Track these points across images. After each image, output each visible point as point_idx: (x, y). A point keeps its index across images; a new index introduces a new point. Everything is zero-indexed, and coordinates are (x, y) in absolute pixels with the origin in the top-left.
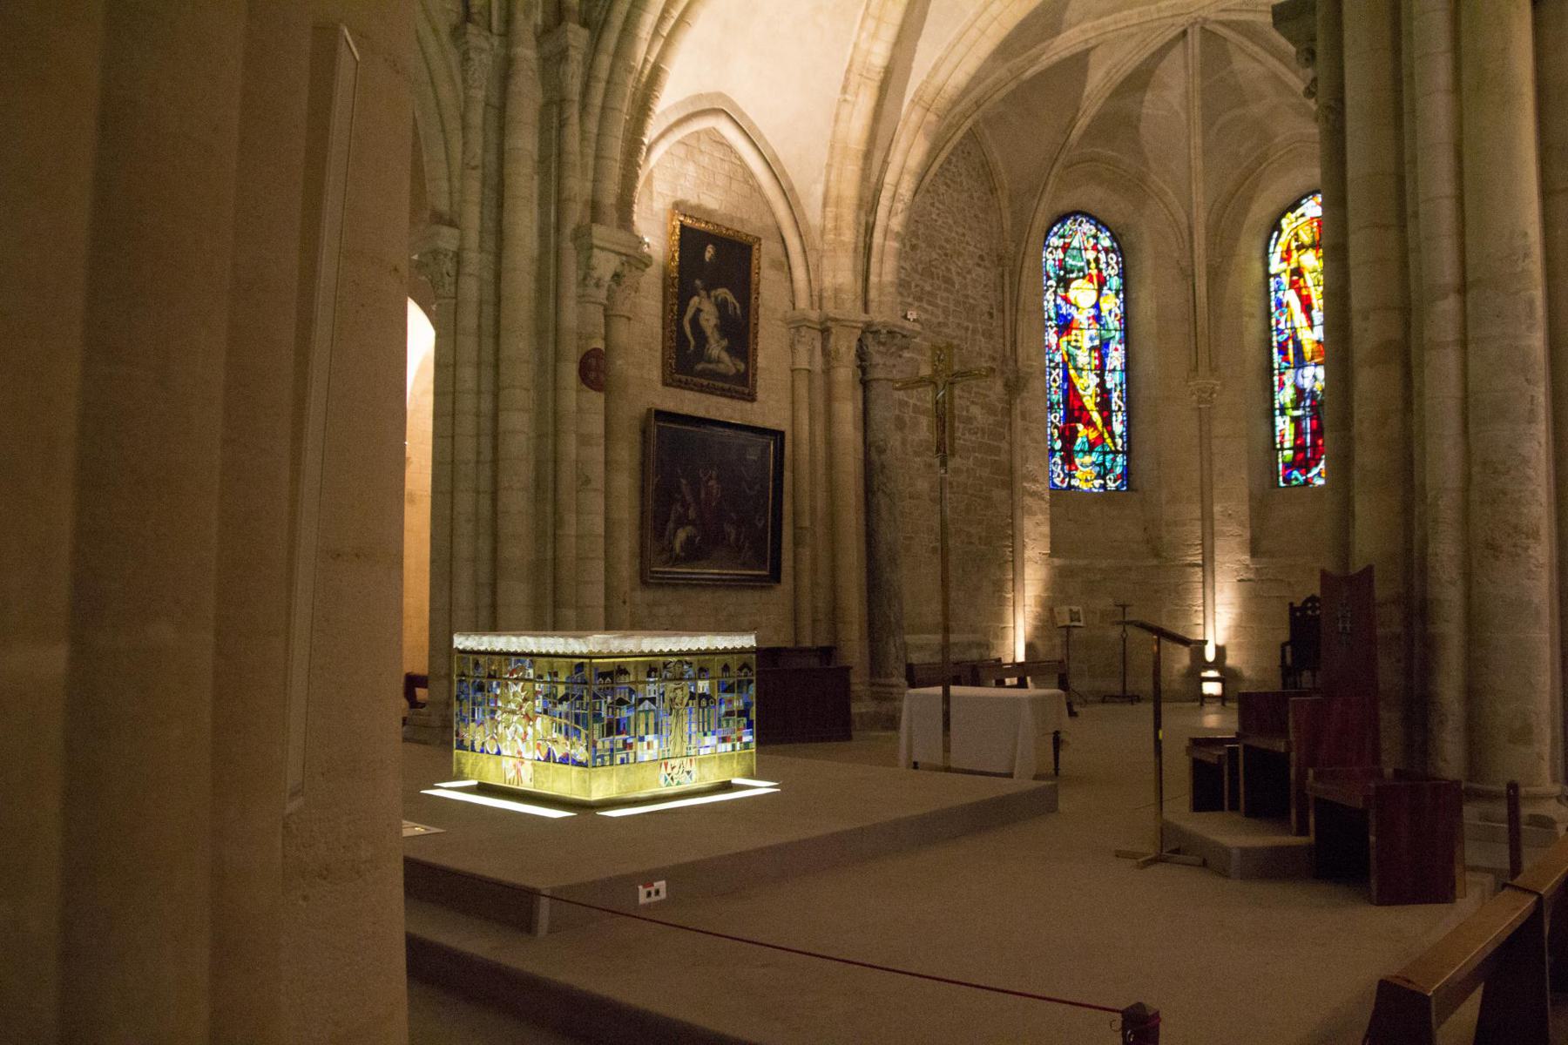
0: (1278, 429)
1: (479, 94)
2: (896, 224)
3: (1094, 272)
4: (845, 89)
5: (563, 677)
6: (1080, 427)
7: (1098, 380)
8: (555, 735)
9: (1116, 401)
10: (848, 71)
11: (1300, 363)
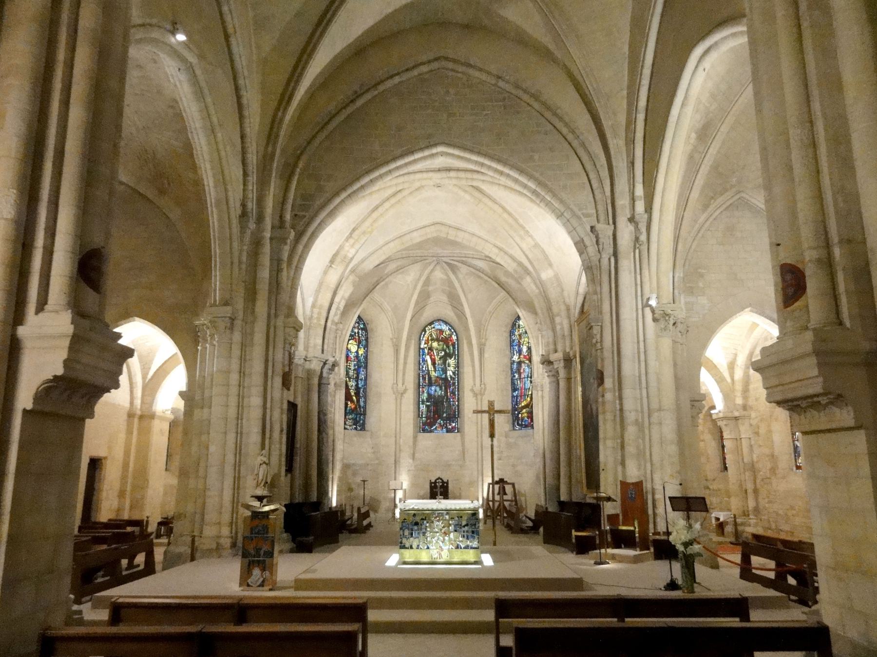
0: (421, 409)
1: (245, 248)
2: (337, 319)
3: (357, 338)
4: (332, 261)
5: (465, 517)
6: (349, 403)
7: (356, 383)
8: (461, 539)
10: (335, 255)
11: (430, 384)
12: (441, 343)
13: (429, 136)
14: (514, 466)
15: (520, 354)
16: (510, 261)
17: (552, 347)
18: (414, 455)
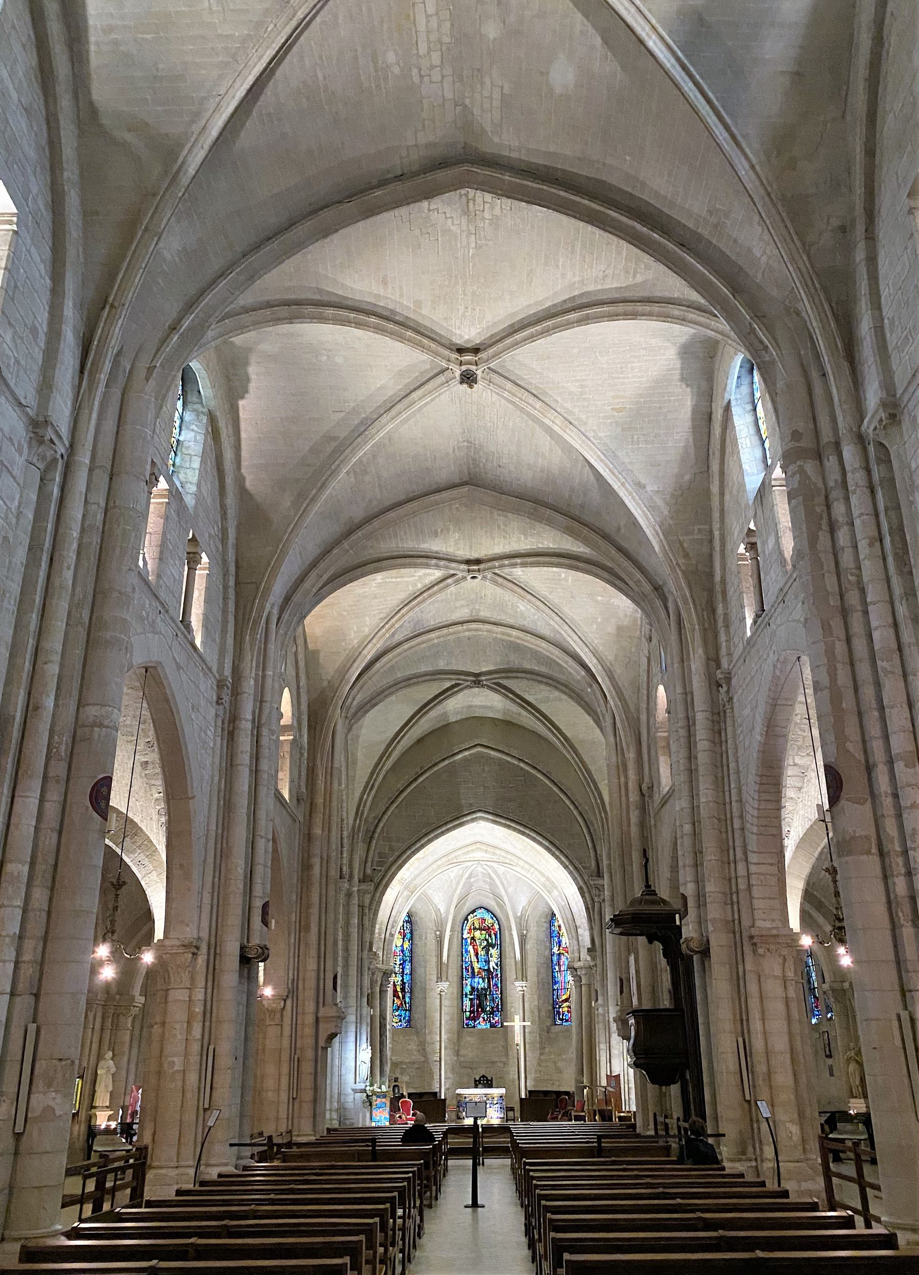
9: (407, 988)
11: (473, 976)
12: (484, 932)
13: (471, 805)
14: (555, 1063)
15: (560, 946)
16: (539, 876)
17: (577, 955)
18: (458, 1051)
